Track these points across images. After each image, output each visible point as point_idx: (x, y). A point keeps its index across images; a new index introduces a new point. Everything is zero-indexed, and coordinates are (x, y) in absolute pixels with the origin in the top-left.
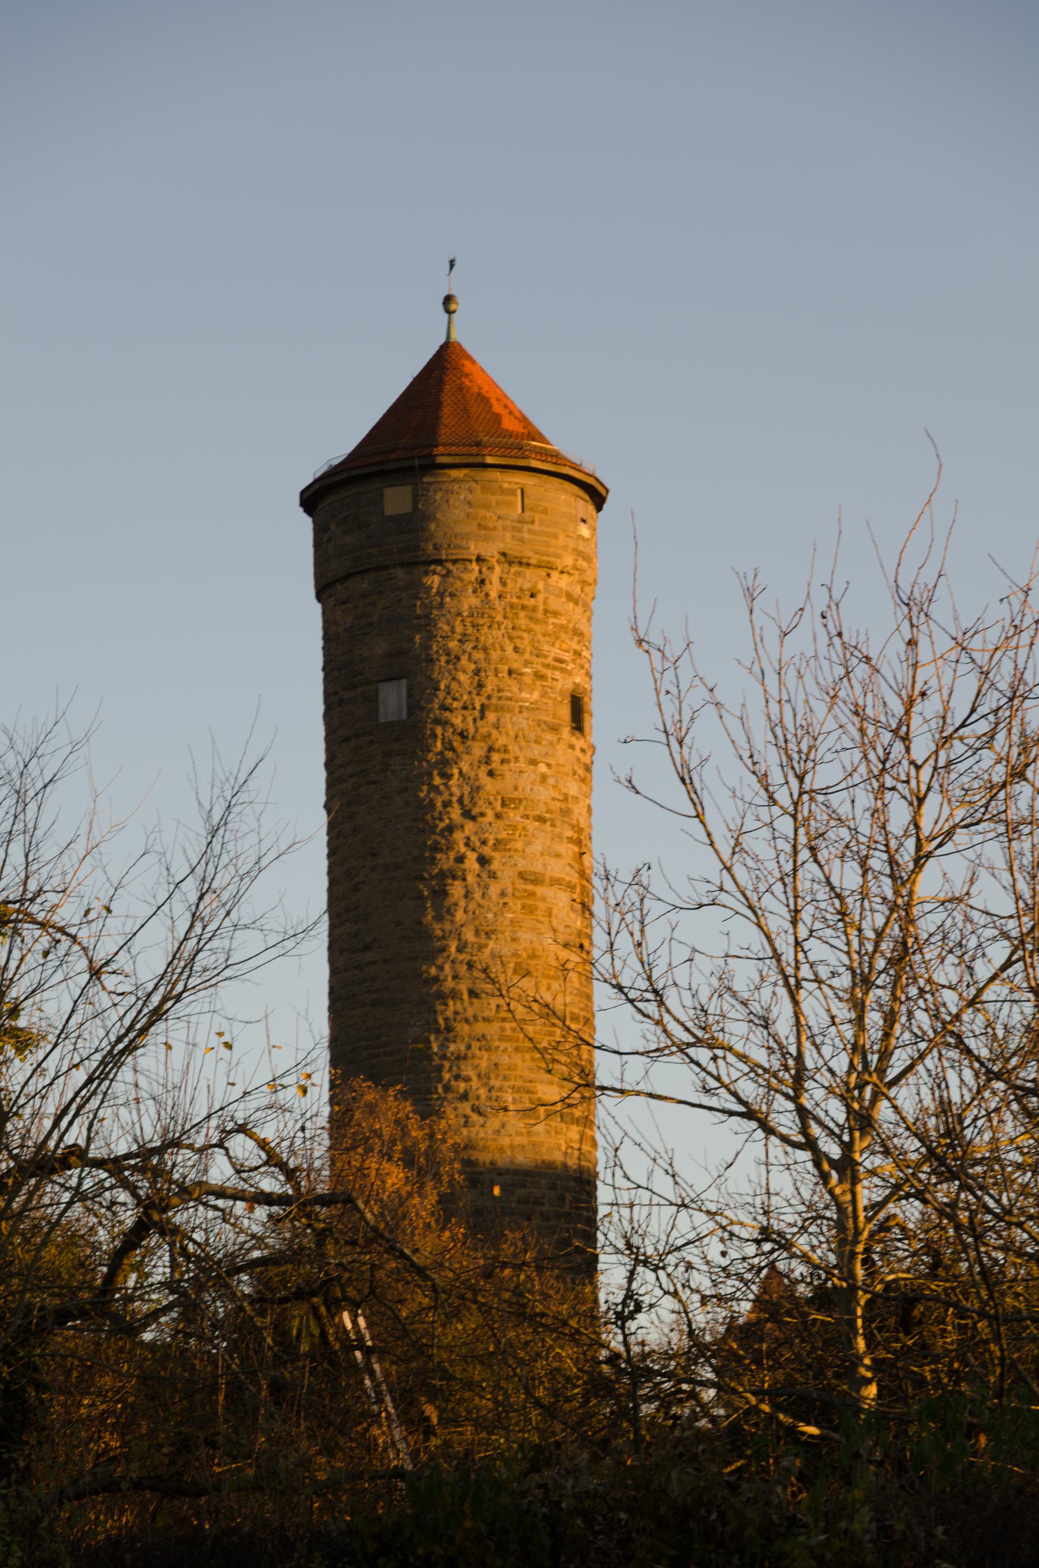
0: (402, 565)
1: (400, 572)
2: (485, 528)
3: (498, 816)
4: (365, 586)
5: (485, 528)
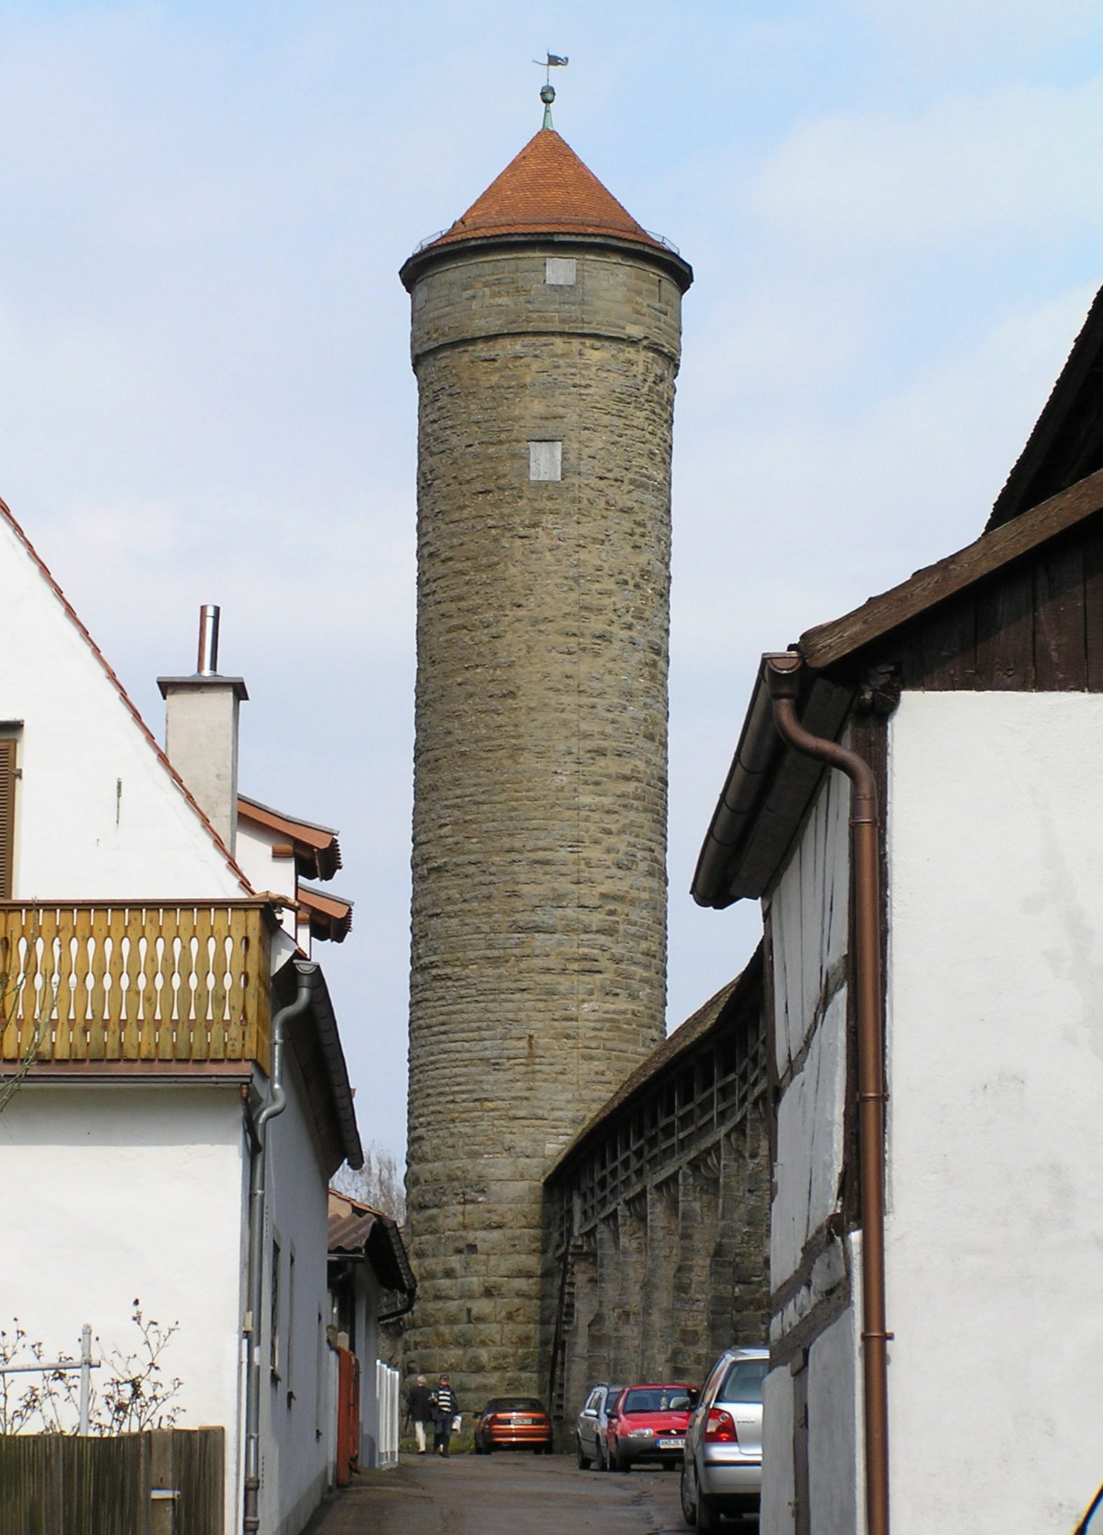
0: (561, 334)
1: (558, 341)
2: (638, 313)
3: (637, 586)
4: (518, 347)
5: (638, 313)
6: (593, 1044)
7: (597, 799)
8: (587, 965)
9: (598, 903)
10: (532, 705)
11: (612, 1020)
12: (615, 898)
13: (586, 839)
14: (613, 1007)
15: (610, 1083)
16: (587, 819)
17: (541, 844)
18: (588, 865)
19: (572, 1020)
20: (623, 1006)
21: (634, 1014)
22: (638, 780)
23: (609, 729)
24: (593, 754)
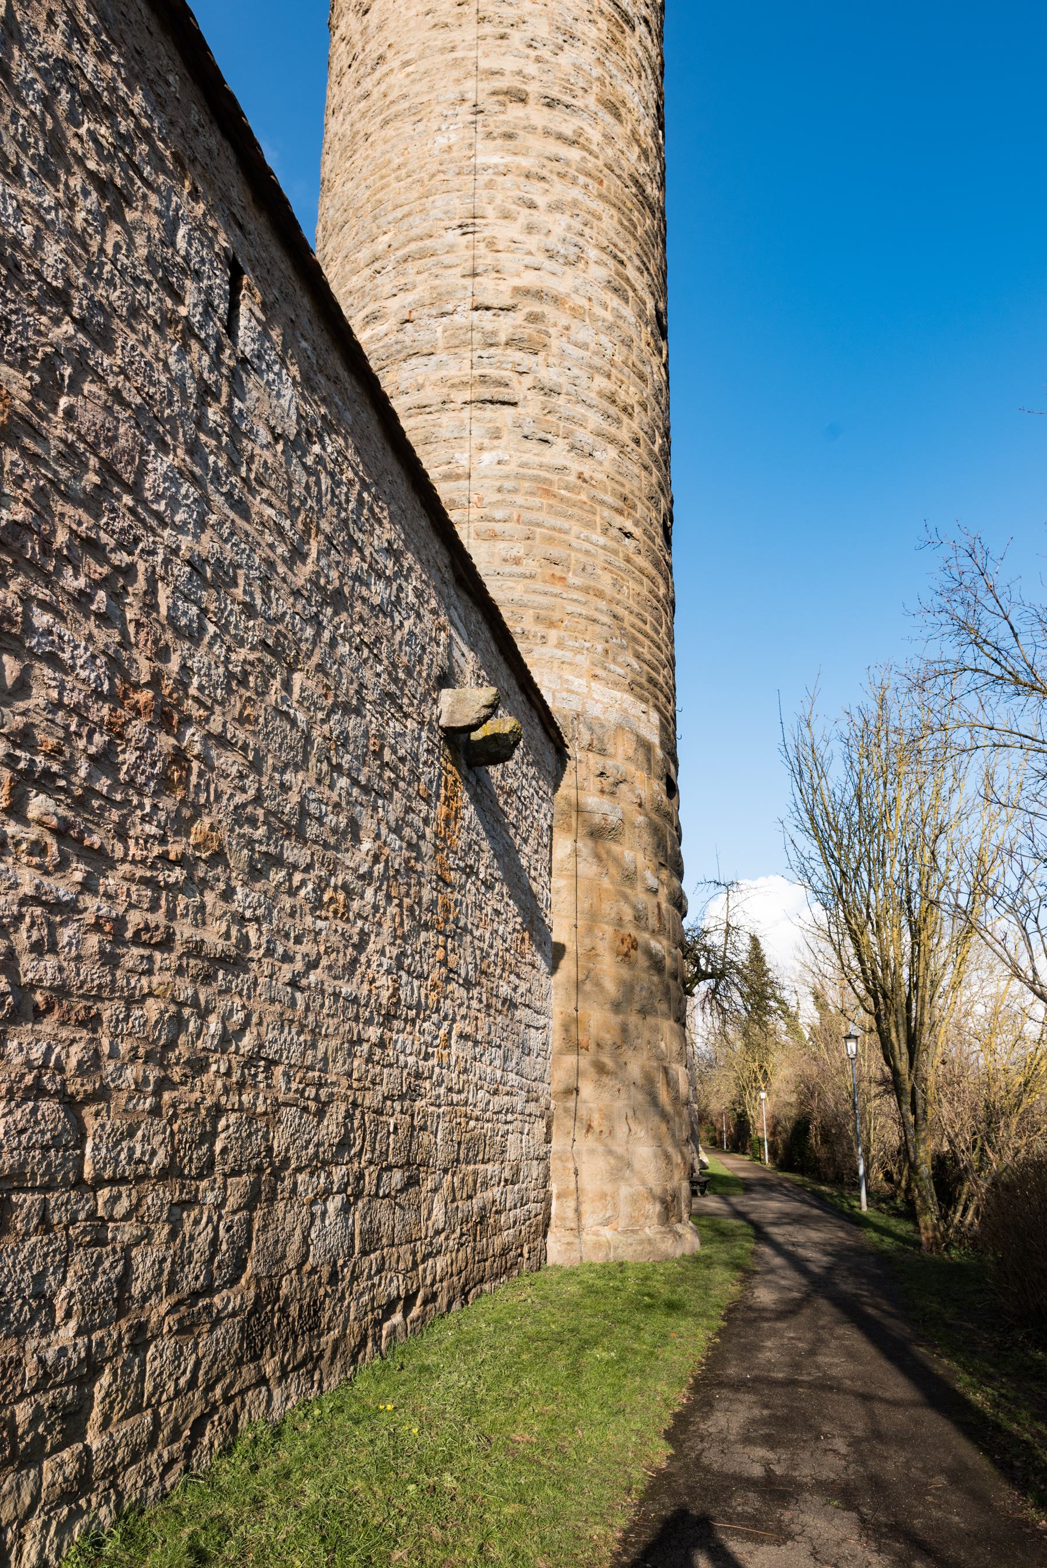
6: (499, 514)
7: (509, 159)
8: (487, 393)
9: (508, 302)
10: (408, 57)
11: (536, 479)
12: (539, 295)
13: (490, 212)
14: (537, 460)
15: (532, 577)
16: (490, 185)
17: (414, 233)
18: (491, 244)
19: (458, 477)
20: (559, 462)
21: (580, 476)
22: (584, 148)
23: (532, 69)
24: (501, 98)
